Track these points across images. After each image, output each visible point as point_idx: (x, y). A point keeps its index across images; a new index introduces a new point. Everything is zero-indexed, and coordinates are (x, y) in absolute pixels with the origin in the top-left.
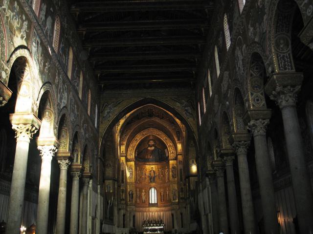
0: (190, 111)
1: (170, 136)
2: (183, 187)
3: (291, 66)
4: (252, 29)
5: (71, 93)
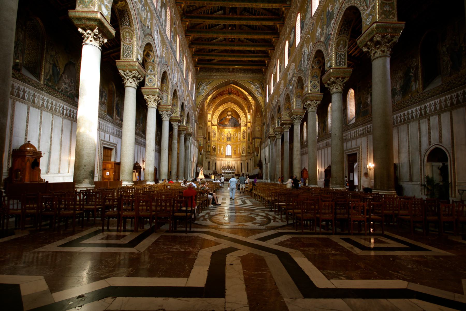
0: (260, 91)
1: (242, 109)
2: (250, 145)
3: (345, 63)
4: (320, 30)
5: (179, 73)
